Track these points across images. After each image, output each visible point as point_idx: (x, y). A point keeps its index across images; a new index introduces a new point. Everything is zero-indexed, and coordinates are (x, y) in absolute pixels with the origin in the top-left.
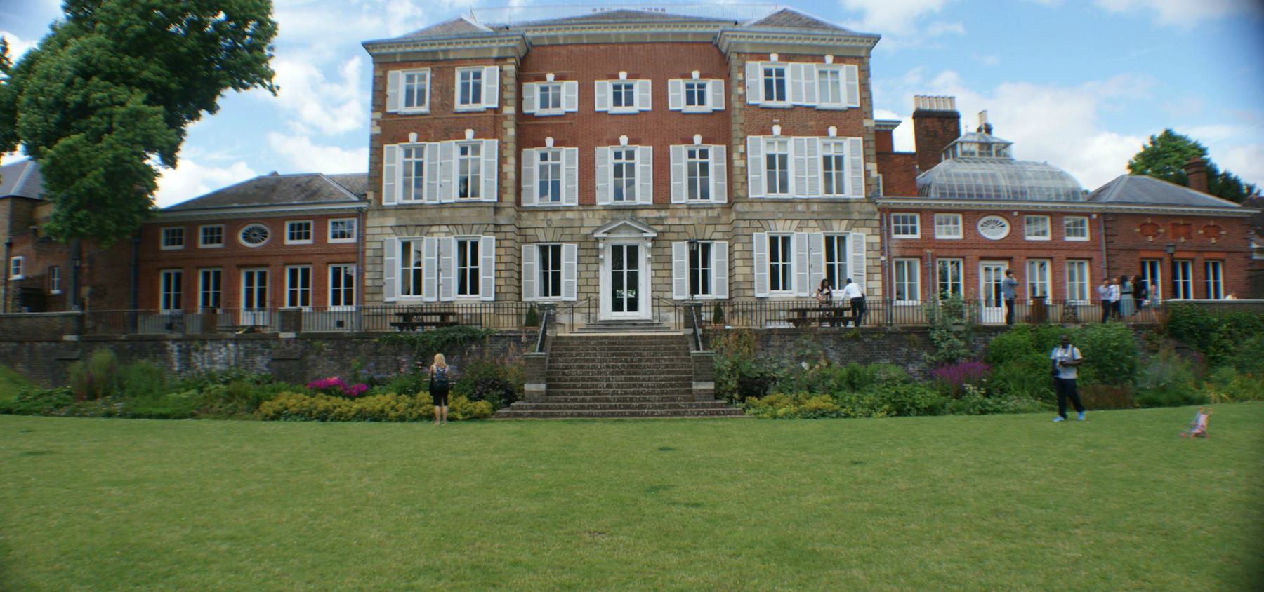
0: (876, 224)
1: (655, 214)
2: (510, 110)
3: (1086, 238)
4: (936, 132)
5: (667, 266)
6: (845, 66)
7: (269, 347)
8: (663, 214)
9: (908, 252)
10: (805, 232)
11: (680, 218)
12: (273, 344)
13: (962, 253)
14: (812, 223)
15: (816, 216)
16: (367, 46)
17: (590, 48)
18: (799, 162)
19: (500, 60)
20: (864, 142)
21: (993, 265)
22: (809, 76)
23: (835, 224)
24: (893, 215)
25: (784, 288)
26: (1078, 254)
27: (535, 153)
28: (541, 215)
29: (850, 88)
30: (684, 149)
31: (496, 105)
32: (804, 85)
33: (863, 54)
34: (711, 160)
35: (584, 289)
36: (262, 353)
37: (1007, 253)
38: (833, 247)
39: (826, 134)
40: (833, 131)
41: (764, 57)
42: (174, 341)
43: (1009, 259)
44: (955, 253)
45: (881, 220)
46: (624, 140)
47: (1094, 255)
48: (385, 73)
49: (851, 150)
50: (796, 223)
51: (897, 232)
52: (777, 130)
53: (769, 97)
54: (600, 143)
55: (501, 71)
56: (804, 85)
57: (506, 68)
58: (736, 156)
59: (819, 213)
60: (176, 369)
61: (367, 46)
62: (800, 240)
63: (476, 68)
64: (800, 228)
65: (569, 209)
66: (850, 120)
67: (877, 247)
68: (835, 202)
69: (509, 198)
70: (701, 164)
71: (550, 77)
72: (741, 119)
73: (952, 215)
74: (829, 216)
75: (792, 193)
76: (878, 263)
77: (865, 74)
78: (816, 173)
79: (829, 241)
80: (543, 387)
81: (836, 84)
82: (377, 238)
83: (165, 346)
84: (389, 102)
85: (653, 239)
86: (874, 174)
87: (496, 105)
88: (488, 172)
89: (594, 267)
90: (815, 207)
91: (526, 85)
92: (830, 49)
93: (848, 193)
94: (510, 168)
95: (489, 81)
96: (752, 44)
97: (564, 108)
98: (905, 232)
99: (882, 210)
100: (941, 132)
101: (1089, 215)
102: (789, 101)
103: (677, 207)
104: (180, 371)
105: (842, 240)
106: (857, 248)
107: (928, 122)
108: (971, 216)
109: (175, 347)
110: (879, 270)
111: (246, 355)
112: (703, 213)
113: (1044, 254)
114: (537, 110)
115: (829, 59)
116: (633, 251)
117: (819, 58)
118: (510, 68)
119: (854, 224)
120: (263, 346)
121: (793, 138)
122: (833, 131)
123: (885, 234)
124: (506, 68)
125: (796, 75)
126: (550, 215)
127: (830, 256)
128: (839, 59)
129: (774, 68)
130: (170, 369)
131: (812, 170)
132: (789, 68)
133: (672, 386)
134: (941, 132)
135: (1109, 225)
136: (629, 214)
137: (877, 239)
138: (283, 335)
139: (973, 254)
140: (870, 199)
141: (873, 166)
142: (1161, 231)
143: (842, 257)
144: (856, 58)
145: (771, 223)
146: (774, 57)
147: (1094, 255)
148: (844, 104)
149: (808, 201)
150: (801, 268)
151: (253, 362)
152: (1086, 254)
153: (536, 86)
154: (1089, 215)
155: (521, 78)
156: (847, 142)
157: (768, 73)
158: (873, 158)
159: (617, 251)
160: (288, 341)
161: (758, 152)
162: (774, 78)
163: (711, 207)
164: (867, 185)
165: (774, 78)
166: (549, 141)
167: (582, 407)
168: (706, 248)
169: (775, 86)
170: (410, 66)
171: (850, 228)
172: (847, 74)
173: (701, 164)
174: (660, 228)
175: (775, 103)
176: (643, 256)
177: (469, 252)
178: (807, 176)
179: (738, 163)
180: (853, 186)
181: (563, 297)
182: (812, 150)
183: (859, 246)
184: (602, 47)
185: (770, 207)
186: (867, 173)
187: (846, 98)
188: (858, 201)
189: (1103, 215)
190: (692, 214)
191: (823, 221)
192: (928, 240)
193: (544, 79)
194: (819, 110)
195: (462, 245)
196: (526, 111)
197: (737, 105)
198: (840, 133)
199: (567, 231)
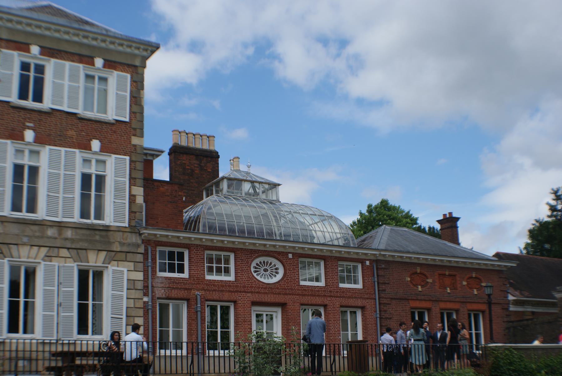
0: (140, 258)
3: (360, 286)
6: (116, 73)
9: (174, 294)
10: (55, 263)
13: (234, 297)
14: (64, 252)
15: (69, 245)
18: (53, 178)
20: (131, 161)
21: (265, 311)
22: (74, 77)
23: (92, 256)
24: (159, 249)
25: (25, 332)
26: (351, 302)
29: (119, 98)
32: (65, 87)
33: (137, 63)
38: (88, 284)
39: (87, 147)
40: (96, 145)
41: (23, 47)
43: (283, 305)
44: (226, 296)
45: (145, 255)
47: (368, 304)
49: (115, 170)
50: (44, 251)
51: (163, 270)
52: (29, 135)
53: (23, 95)
56: (65, 87)
59: (72, 240)
62: (48, 272)
64: (48, 257)
66: (119, 136)
67: (140, 285)
68: (92, 228)
73: (223, 254)
75: (42, 213)
76: (140, 304)
77: (138, 84)
78: (73, 192)
79: (83, 275)
81: (104, 93)
86: (140, 200)
90: (69, 233)
92: (101, 52)
93: (109, 219)
96: (10, 30)
98: (172, 270)
99: (147, 242)
100: (197, 171)
101: (362, 262)
102: (47, 104)
105: (98, 275)
106: (116, 286)
108: (245, 255)
110: (141, 312)
113: (319, 300)
115: (99, 62)
117: (88, 60)
119: (114, 256)
121: (48, 147)
122: (96, 145)
123: (149, 272)
125: (58, 74)
127: (83, 294)
128: (110, 64)
129: (32, 62)
134: (197, 171)
135: (381, 273)
137: (140, 276)
139: (245, 298)
140: (133, 229)
141: (139, 191)
142: (430, 280)
143: (98, 295)
144: (129, 66)
145: (14, 248)
146: (35, 49)
147: (368, 304)
148: (111, 115)
149: (60, 225)
150: (47, 306)
152: (359, 303)
156: (111, 160)
157: (25, 67)
158: (140, 182)
162: (32, 74)
164: (131, 212)
165: (32, 74)
171: (108, 261)
172: (117, 83)
175: (29, 103)
178: (61, 195)
180: (115, 211)
182: (70, 165)
183: (118, 283)
185: (14, 229)
186: (132, 198)
187: (115, 110)
188: (119, 230)
189: (376, 262)
191: (77, 251)
192: (197, 280)
194: (82, 119)
198: (104, 149)
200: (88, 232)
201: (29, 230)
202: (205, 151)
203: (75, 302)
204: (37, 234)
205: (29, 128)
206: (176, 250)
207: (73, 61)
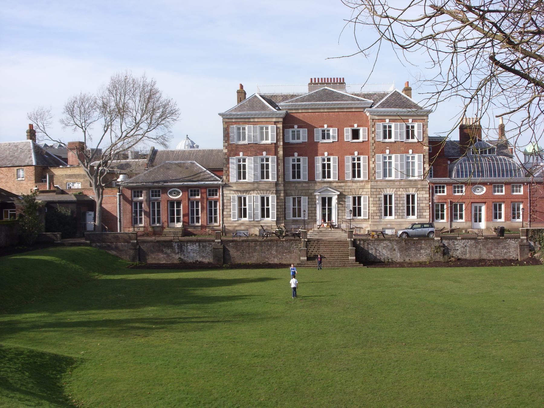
0: (428, 189)
1: (340, 184)
7: (211, 244)
8: (342, 184)
9: (440, 201)
11: (349, 186)
12: (213, 244)
13: (464, 201)
16: (220, 114)
19: (275, 123)
23: (411, 189)
26: (516, 200)
27: (291, 158)
28: (293, 185)
30: (350, 157)
31: (275, 142)
35: (310, 215)
37: (484, 201)
44: (461, 201)
46: (326, 154)
48: (228, 127)
55: (277, 127)
58: (371, 162)
61: (220, 114)
65: (305, 182)
69: (281, 179)
70: (358, 163)
71: (296, 126)
74: (408, 187)
79: (408, 196)
80: (306, 258)
82: (228, 195)
84: (231, 139)
85: (338, 195)
87: (275, 142)
88: (273, 170)
89: (314, 206)
94: (281, 168)
95: (272, 132)
97: (301, 141)
101: (523, 183)
102: (393, 140)
103: (346, 182)
104: (178, 253)
111: (203, 247)
112: (358, 184)
114: (291, 141)
116: (330, 199)
118: (280, 126)
119: (418, 190)
125: (396, 128)
126: (297, 185)
127: (408, 203)
132: (393, 125)
137: (428, 196)
138: (216, 241)
145: (385, 189)
146: (387, 121)
152: (520, 200)
153: (291, 130)
154: (523, 183)
155: (284, 128)
157: (385, 127)
159: (324, 199)
160: (218, 242)
162: (387, 129)
165: (387, 129)
166: (296, 154)
168: (359, 198)
169: (387, 133)
170: (239, 124)
173: (358, 163)
174: (341, 190)
175: (387, 140)
176: (334, 201)
177: (264, 201)
179: (372, 166)
181: (302, 218)
184: (317, 114)
185: (385, 183)
186: (424, 169)
190: (354, 184)
193: (294, 128)
195: (263, 198)
197: (372, 141)
199: (304, 191)
201: (389, 183)
203: (405, 205)
206: (442, 185)
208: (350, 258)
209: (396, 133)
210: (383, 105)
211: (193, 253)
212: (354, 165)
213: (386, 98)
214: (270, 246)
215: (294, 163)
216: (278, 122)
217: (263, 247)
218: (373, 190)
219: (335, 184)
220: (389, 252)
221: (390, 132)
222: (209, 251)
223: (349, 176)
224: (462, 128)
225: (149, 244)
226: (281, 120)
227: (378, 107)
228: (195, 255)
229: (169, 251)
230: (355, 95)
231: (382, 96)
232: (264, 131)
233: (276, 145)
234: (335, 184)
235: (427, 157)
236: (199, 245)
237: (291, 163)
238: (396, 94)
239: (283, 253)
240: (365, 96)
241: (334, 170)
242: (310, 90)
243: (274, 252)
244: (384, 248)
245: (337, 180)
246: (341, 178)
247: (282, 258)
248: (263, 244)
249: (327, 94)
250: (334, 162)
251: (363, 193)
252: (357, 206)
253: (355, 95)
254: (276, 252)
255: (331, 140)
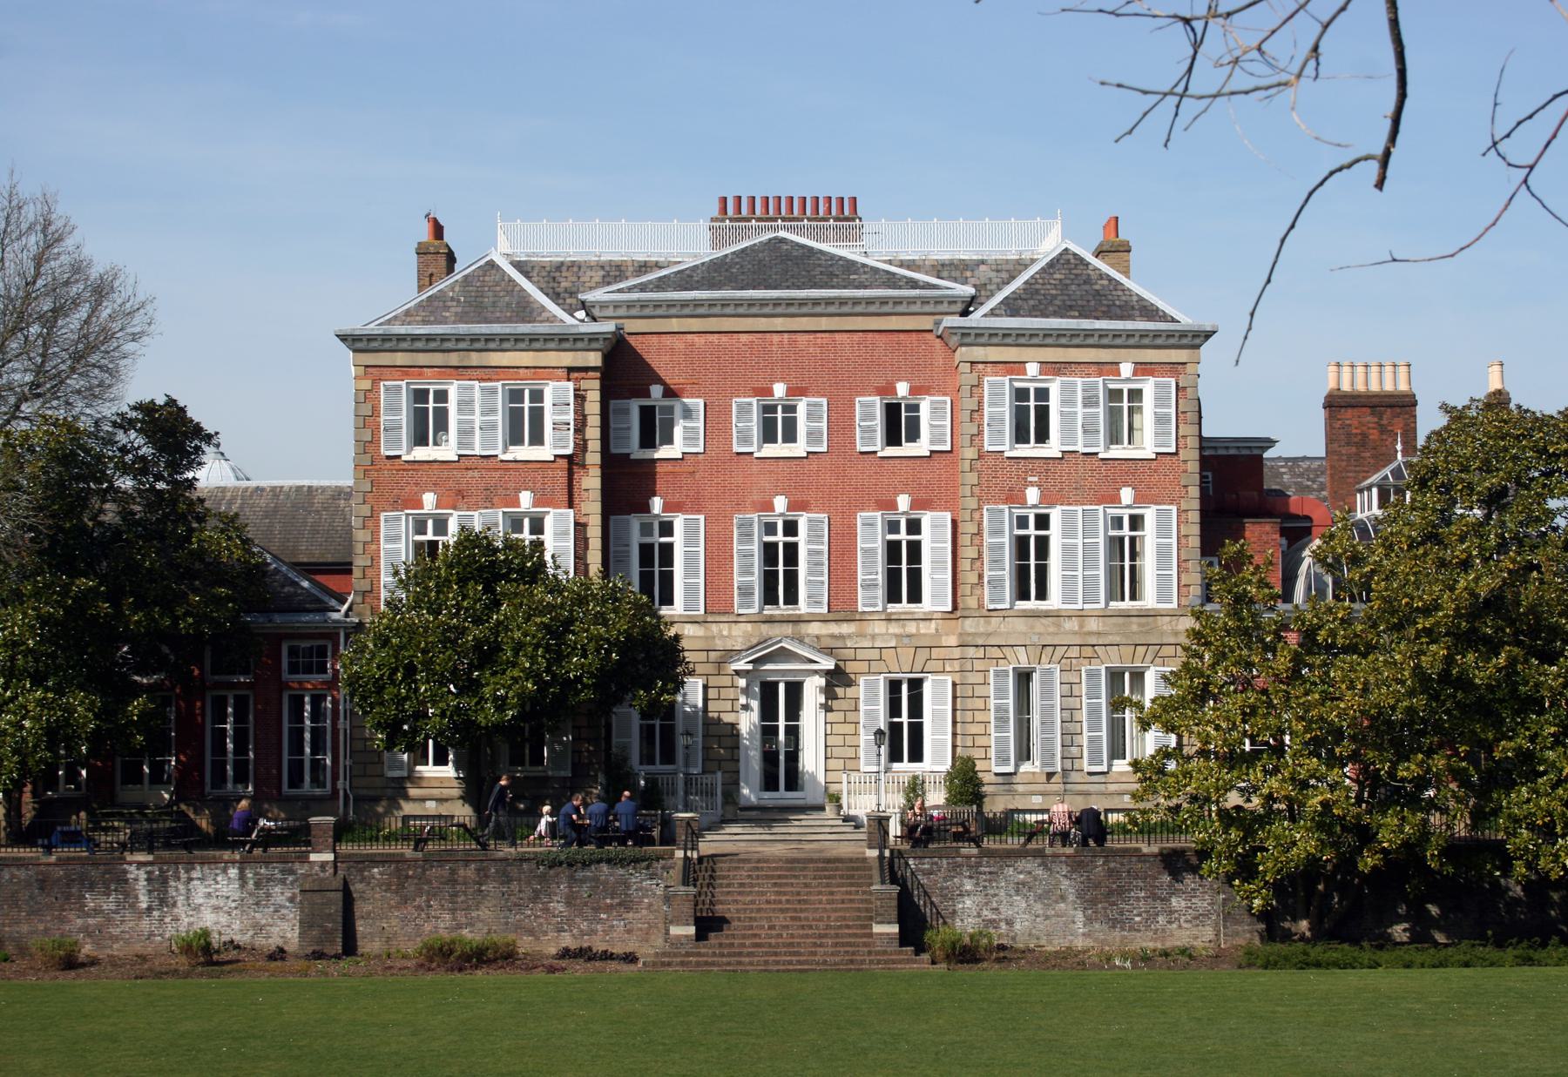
1: (834, 629)
2: (593, 458)
4: (1364, 436)
5: (851, 716)
6: (1152, 380)
7: (292, 872)
8: (846, 628)
11: (873, 637)
17: (724, 338)
18: (1068, 551)
27: (635, 522)
29: (1161, 420)
31: (569, 451)
34: (925, 537)
36: (283, 882)
42: (140, 864)
46: (780, 503)
53: (1021, 436)
54: (739, 507)
57: (584, 384)
60: (144, 905)
63: (536, 384)
68: (1126, 615)
72: (972, 478)
80: (692, 930)
83: (125, 872)
85: (828, 673)
91: (613, 403)
93: (1149, 600)
100: (1374, 435)
102: (1053, 448)
104: (150, 909)
107: (1349, 416)
109: (142, 875)
111: (257, 885)
112: (911, 628)
116: (795, 691)
120: (282, 872)
121: (1059, 508)
124: (584, 384)
128: (1143, 369)
130: (133, 906)
131: (1089, 562)
133: (848, 927)
134: (1374, 435)
136: (788, 629)
149: (1081, 615)
151: (268, 895)
153: (635, 406)
157: (1021, 394)
160: (323, 865)
161: (999, 532)
162: (1032, 403)
163: (927, 619)
167: (740, 954)
168: (916, 685)
169: (1031, 421)
170: (420, 375)
178: (1080, 573)
184: (744, 338)
185: (1020, 625)
193: (647, 395)
196: (614, 450)
200: (1121, 620)
202: (1390, 396)
204: (1051, 630)
205: (1032, 484)
207: (1089, 375)
208: (877, 929)
209: (1068, 419)
210: (1011, 307)
211: (216, 909)
212: (893, 549)
213: (1025, 276)
214: (543, 878)
215: (648, 540)
216: (586, 369)
217: (515, 886)
218: (971, 652)
219: (814, 629)
220: (1038, 908)
221: (1043, 414)
222: (281, 900)
223: (870, 597)
224: (1336, 404)
225: (22, 874)
226: (594, 359)
227: (992, 313)
228: (224, 919)
229: (109, 904)
230: (902, 264)
231: (1013, 269)
232: (527, 404)
233: (573, 463)
234: (814, 629)
235: (1195, 517)
236: (242, 878)
237: (636, 539)
238: (1066, 262)
239: (597, 910)
240: (940, 269)
241: (690, 570)
242: (717, 240)
243: (558, 907)
244: (1019, 887)
245: (825, 610)
246: (841, 607)
247: (593, 932)
248: (513, 871)
249: (787, 257)
250: (814, 537)
251: (930, 666)
252: (904, 719)
253: (902, 264)
254: (568, 904)
255: (799, 448)
